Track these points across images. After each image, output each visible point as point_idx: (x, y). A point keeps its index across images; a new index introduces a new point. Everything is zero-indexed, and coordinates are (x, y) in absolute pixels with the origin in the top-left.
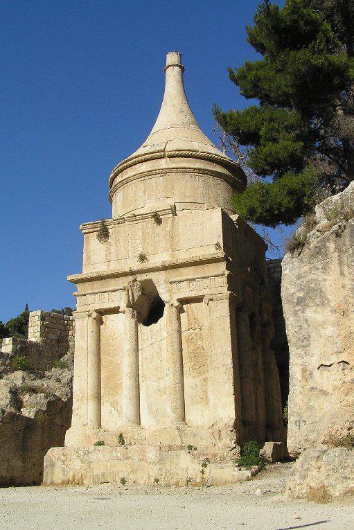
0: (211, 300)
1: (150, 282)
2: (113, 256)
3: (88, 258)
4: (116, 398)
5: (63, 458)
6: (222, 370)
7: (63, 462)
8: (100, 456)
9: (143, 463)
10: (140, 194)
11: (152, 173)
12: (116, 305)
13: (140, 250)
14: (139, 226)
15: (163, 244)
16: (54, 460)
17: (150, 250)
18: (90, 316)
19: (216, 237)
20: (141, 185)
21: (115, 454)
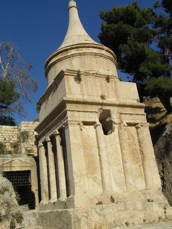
0: (142, 126)
1: (109, 111)
2: (85, 92)
3: (69, 89)
4: (95, 175)
5: (86, 215)
6: (152, 160)
7: (87, 217)
8: (111, 210)
9: (136, 211)
10: (94, 63)
11: (101, 55)
12: (92, 120)
13: (100, 93)
14: (98, 80)
15: (112, 93)
16: (80, 217)
17: (106, 94)
18: (79, 124)
19: (136, 97)
20: (94, 59)
21: (119, 208)
